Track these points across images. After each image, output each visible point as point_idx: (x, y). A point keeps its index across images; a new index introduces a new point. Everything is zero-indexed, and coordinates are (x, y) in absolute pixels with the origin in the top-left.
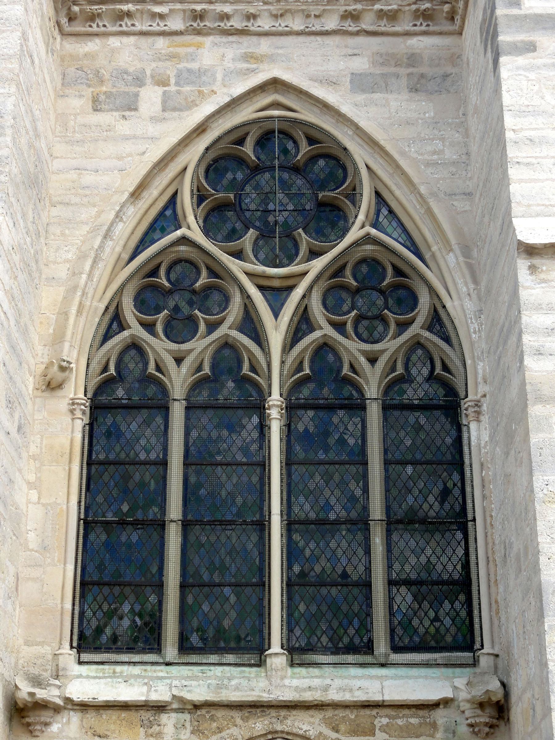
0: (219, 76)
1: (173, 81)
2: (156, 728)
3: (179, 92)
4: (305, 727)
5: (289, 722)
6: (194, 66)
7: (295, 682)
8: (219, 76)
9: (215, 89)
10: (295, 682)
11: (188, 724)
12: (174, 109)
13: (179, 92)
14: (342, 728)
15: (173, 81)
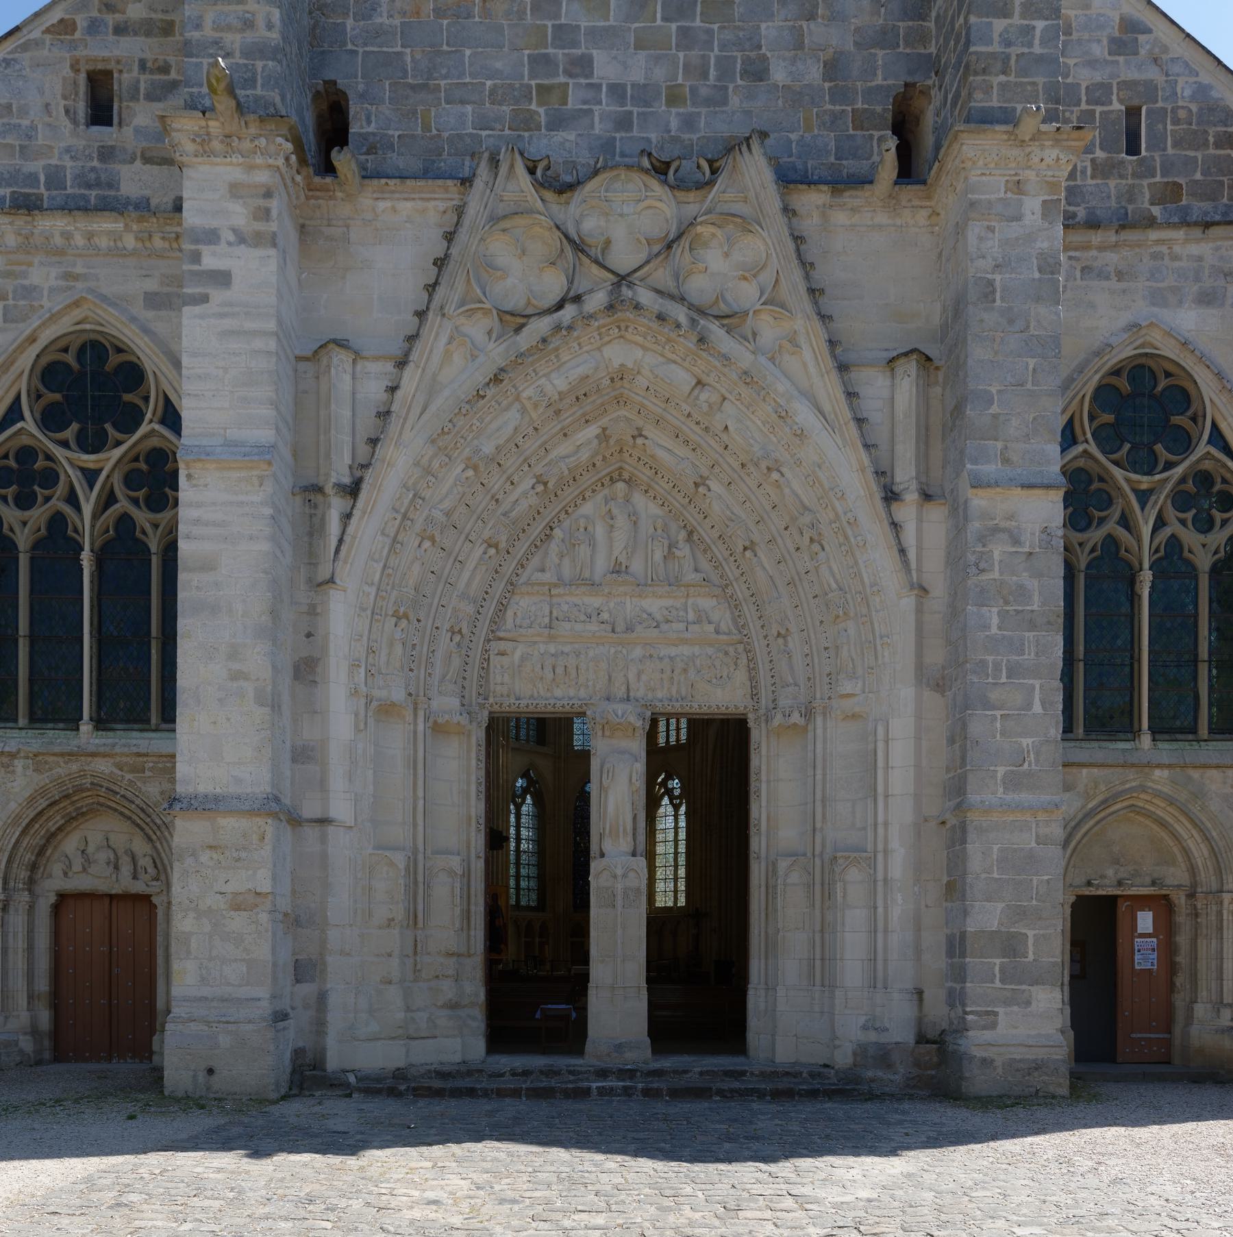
0: (46, 293)
1: (10, 296)
2: (11, 768)
3: (15, 306)
4: (103, 768)
5: (93, 765)
6: (26, 282)
7: (97, 741)
8: (46, 293)
9: (42, 303)
10: (97, 741)
11: (31, 766)
12: (13, 321)
13: (15, 306)
14: (125, 768)
15: (10, 296)
